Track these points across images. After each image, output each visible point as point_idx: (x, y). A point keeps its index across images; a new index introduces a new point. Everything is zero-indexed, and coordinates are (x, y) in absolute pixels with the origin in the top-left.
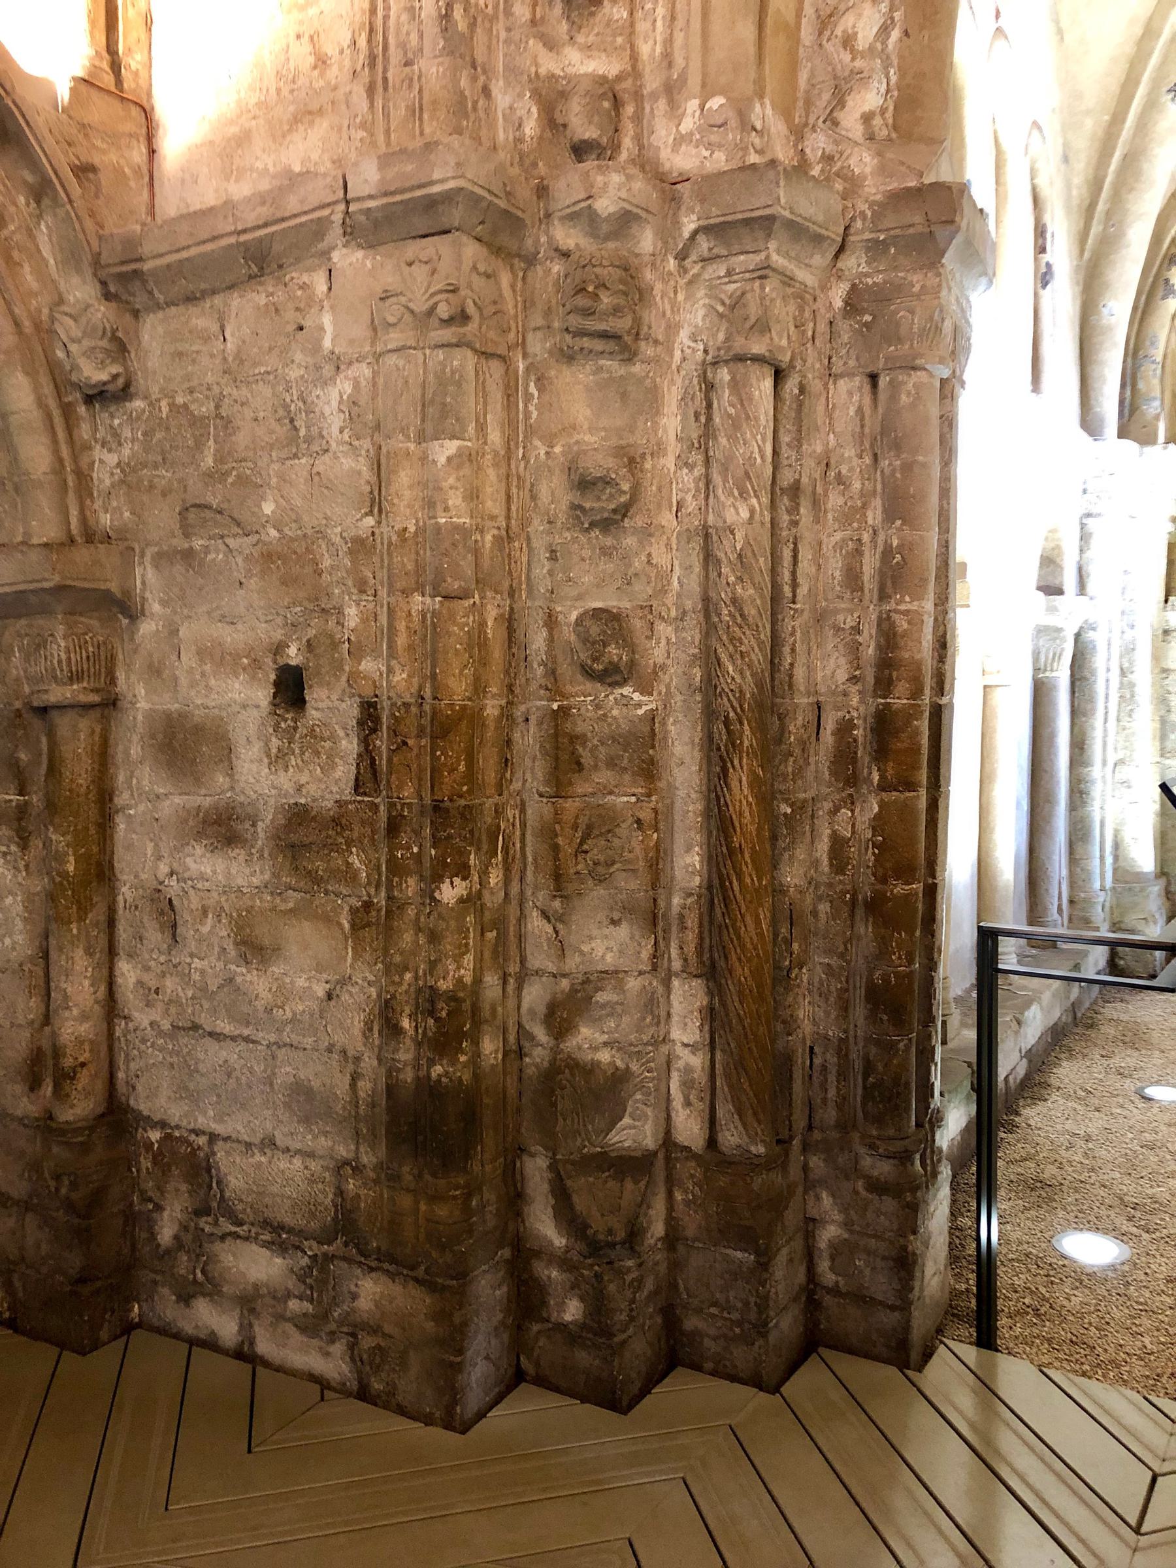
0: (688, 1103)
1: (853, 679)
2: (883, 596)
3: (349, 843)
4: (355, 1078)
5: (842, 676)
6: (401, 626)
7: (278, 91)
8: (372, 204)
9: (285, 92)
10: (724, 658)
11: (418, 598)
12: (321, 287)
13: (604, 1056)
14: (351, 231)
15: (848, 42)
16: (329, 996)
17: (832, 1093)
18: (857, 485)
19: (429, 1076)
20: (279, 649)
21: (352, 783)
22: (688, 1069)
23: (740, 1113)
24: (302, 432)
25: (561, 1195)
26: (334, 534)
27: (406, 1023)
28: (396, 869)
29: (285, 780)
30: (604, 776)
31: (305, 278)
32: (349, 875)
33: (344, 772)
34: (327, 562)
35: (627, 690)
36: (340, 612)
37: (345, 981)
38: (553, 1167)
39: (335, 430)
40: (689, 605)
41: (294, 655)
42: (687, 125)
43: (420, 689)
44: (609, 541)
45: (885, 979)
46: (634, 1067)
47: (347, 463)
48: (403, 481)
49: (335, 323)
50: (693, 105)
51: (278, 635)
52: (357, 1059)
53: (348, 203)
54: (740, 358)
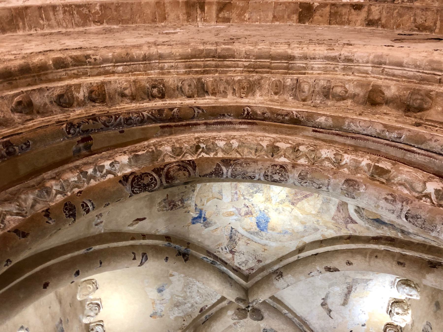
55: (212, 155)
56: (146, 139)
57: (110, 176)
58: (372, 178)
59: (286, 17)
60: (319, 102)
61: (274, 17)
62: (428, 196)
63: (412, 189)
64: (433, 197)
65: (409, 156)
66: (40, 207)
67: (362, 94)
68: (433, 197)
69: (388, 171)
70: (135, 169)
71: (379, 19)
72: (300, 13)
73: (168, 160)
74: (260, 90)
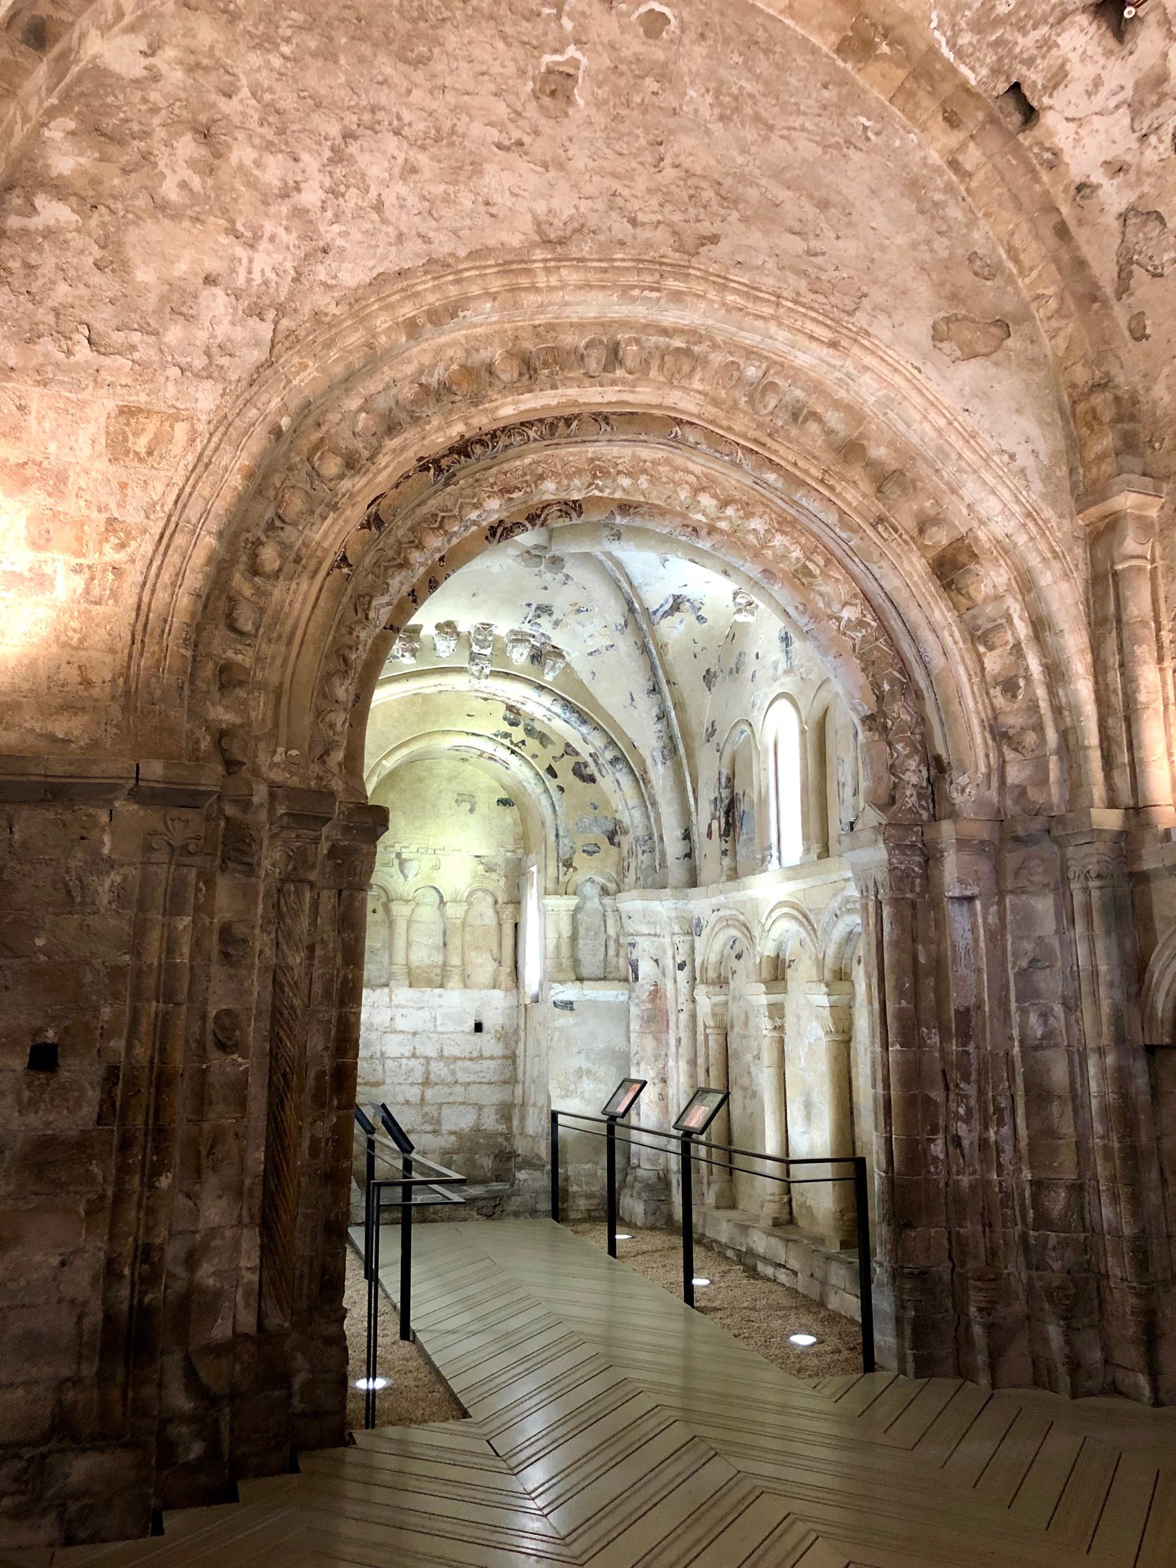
0: (247, 1305)
1: (326, 1048)
2: (342, 1003)
3: (90, 1158)
4: (80, 1319)
5: (320, 1047)
6: (144, 1021)
7: (49, 688)
8: (157, 785)
9: (55, 690)
10: (285, 1038)
11: (154, 1004)
12: (105, 818)
13: (211, 1281)
14: (137, 795)
15: (332, 726)
16: (63, 1264)
17: (305, 1290)
18: (331, 946)
19: (140, 1302)
20: (40, 1031)
21: (95, 1117)
22: (250, 1283)
23: (279, 1303)
24: (79, 900)
25: (191, 1375)
26: (97, 962)
27: (127, 1271)
28: (123, 1170)
29: (33, 1120)
30: (220, 1108)
31: (91, 811)
32: (90, 1178)
33: (88, 1111)
34: (89, 978)
35: (235, 1056)
36: (97, 1010)
37: (80, 1250)
38: (187, 1358)
39: (105, 901)
40: (264, 1007)
41: (51, 1035)
42: (277, 758)
43: (152, 1058)
44: (232, 971)
45: (336, 1216)
46: (226, 1287)
47: (113, 922)
48: (155, 937)
49: (113, 842)
50: (281, 750)
51: (38, 1023)
52: (85, 1304)
53: (137, 779)
54: (301, 881)
55: (605, 495)
56: (519, 456)
57: (474, 528)
58: (795, 573)
59: (815, 22)
60: (780, 423)
61: (790, 6)
62: (839, 619)
63: (828, 605)
64: (843, 623)
65: (847, 561)
66: (406, 589)
67: (842, 434)
68: (843, 623)
69: (814, 576)
70: (504, 515)
71: (970, 175)
72: (845, 39)
73: (546, 497)
74: (704, 369)
